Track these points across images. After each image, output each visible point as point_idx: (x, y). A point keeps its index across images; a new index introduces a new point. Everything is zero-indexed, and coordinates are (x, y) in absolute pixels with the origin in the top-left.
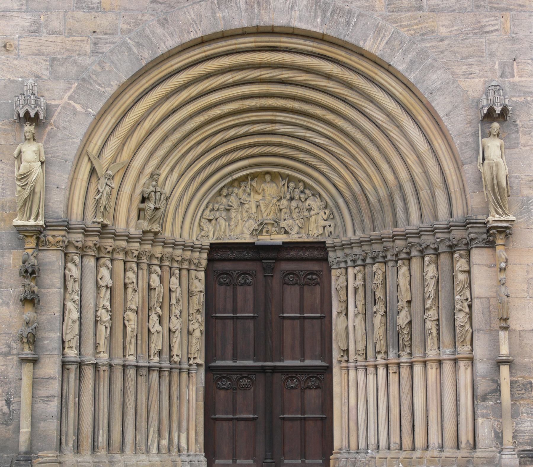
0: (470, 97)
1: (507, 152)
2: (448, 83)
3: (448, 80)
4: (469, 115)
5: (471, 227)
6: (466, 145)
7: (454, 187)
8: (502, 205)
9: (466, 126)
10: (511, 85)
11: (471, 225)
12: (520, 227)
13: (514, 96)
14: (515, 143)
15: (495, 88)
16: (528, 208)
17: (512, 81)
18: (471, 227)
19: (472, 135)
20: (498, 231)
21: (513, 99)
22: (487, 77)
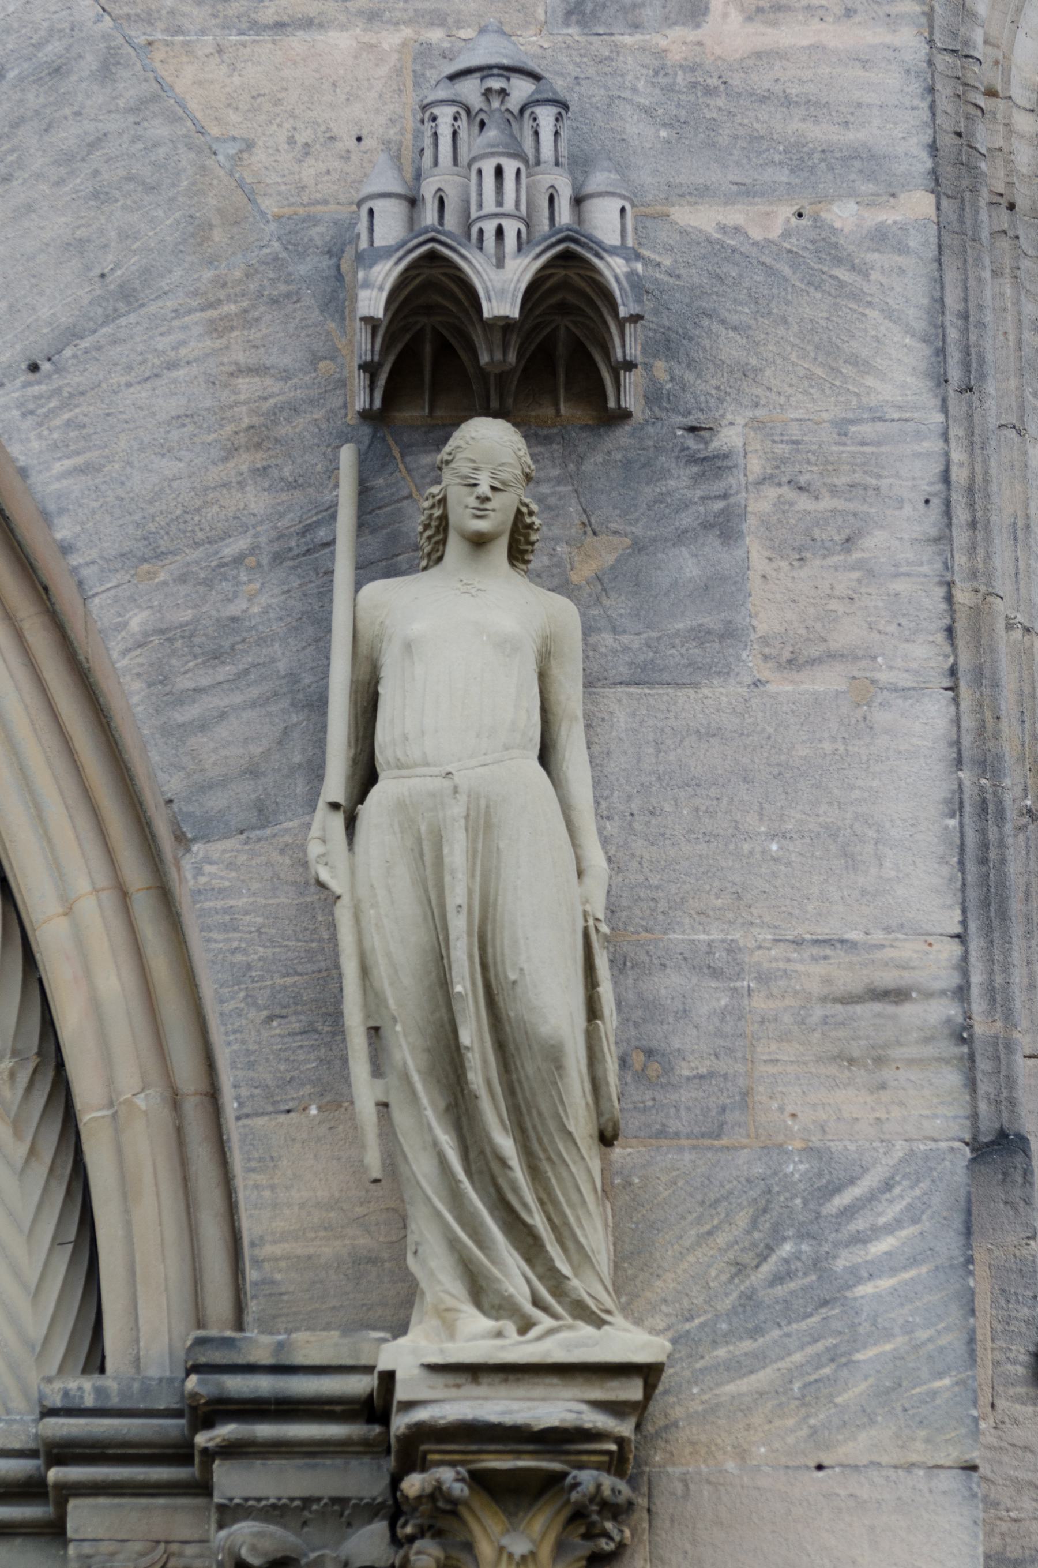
0: (270, 205)
1: (622, 718)
2: (57, 71)
3: (54, 48)
4: (258, 370)
5: (232, 1450)
6: (216, 657)
7: (110, 1082)
8: (537, 1220)
9: (215, 474)
10: (669, 89)
11: (227, 1431)
12: (742, 1454)
13: (701, 193)
14: (701, 635)
15: (488, 93)
16: (816, 1264)
17: (676, 55)
18: (232, 1450)
19: (278, 559)
20: (480, 1480)
21: (684, 216)
22: (438, 19)
